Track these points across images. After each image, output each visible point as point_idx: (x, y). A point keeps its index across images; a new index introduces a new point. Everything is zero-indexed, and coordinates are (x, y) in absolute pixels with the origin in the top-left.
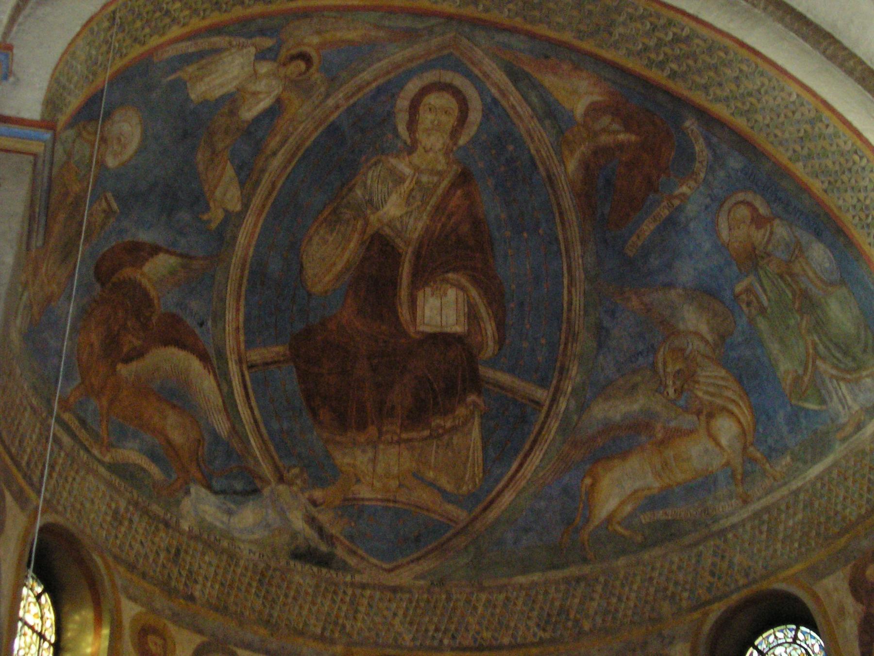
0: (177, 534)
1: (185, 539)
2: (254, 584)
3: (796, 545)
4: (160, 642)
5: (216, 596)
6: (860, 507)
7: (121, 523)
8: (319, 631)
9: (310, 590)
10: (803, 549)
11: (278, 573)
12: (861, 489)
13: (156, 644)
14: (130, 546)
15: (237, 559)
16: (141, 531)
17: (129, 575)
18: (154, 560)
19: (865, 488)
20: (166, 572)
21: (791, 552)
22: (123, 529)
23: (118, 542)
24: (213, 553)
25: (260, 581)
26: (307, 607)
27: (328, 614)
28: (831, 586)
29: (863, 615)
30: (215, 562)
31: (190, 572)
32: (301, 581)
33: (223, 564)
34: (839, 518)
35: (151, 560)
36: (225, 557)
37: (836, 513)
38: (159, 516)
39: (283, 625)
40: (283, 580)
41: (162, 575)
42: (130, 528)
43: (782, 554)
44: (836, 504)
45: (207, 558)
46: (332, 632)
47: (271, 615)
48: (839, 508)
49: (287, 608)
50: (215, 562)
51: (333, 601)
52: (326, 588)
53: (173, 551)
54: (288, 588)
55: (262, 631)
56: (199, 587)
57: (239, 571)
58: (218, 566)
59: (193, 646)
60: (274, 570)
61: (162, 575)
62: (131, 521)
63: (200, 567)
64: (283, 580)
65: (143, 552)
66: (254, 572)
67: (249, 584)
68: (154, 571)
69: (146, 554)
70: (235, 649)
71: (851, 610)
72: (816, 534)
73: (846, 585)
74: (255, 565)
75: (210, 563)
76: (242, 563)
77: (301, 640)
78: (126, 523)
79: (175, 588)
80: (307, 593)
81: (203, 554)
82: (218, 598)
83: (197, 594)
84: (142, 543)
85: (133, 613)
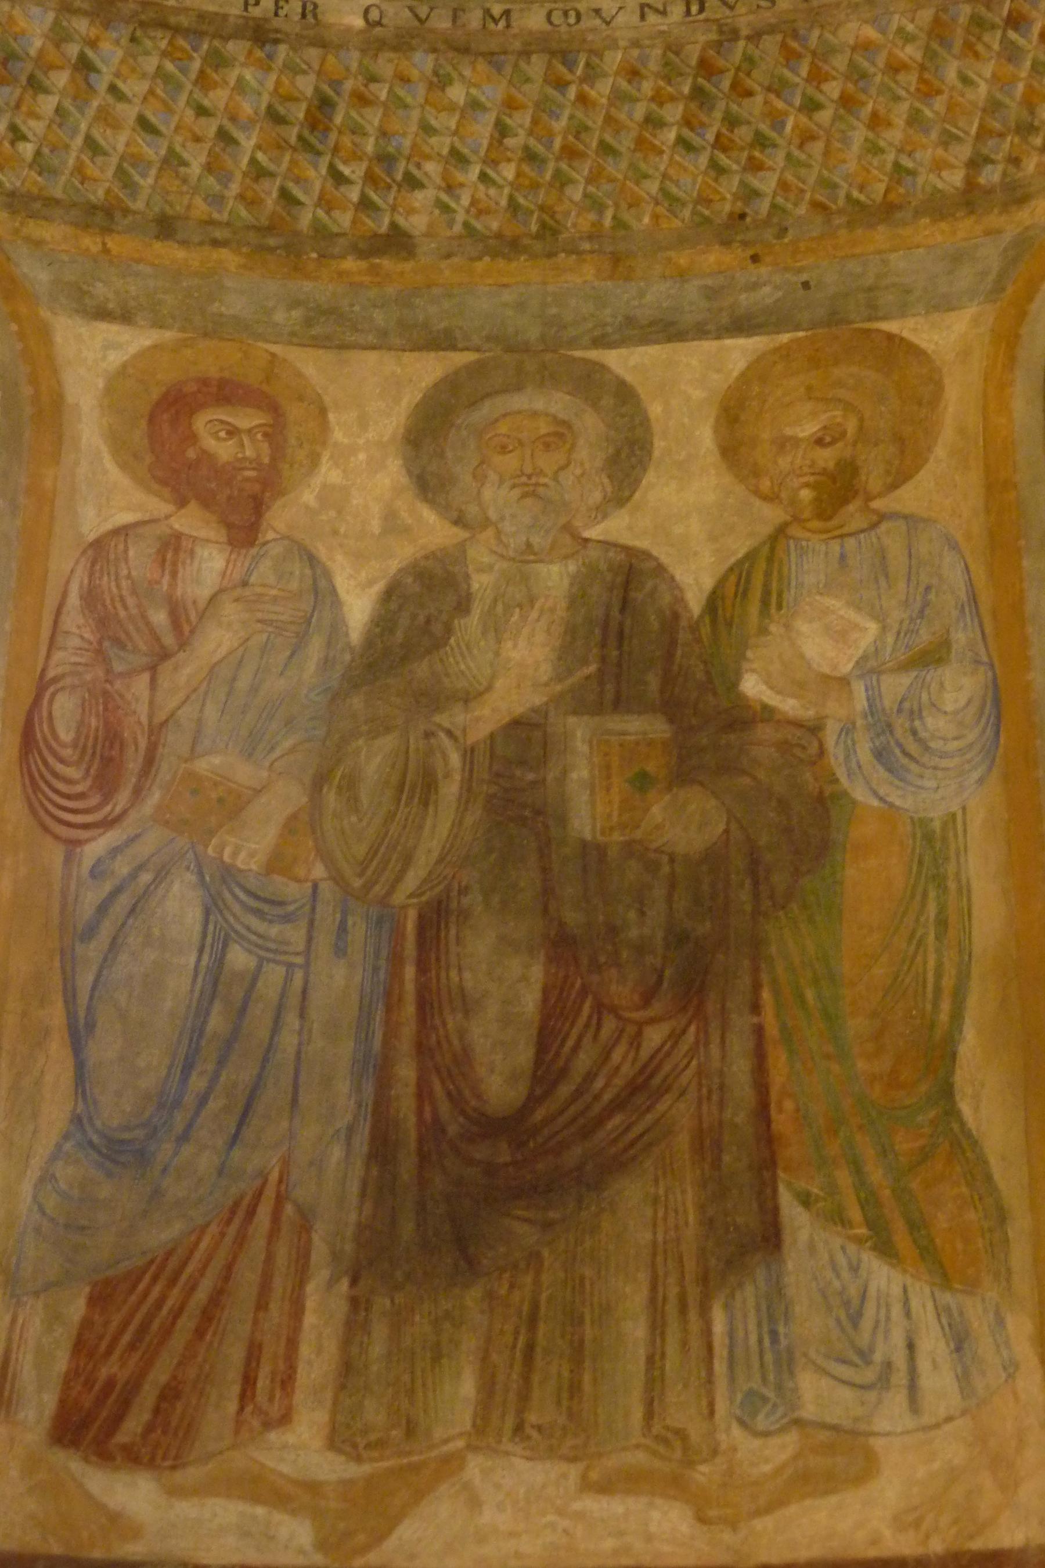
0: (313, 54)
1: (354, 58)
2: (673, 113)
4: (247, 419)
5: (504, 202)
7: (35, 85)
8: (956, 178)
9: (911, 52)
11: (770, 43)
13: (233, 432)
14: (91, 145)
15: (591, 51)
16: (135, 87)
17: (91, 242)
18: (209, 168)
20: (269, 193)
22: (47, 104)
23: (27, 149)
24: (482, 66)
25: (698, 92)
26: (900, 113)
27: (993, 106)
30: (493, 93)
31: (386, 159)
32: (870, 32)
33: (532, 91)
35: (195, 169)
36: (536, 67)
38: (225, 17)
39: (802, 210)
40: (791, 57)
41: (252, 203)
42: (80, 94)
45: (457, 93)
46: (1015, 161)
47: (752, 194)
49: (817, 148)
50: (493, 93)
51: (1011, 54)
52: (978, 22)
53: (299, 112)
54: (817, 77)
55: (714, 257)
56: (420, 198)
57: (601, 91)
58: (511, 105)
59: (410, 399)
60: (755, 37)
61: (252, 203)
62: (84, 66)
63: (427, 129)
64: (791, 57)
65: (152, 151)
66: (670, 72)
67: (653, 122)
68: (217, 200)
69: (171, 150)
70: (593, 354)
74: (674, 48)
75: (475, 105)
76: (614, 59)
77: (881, 235)
78: (61, 79)
79: (319, 231)
80: (895, 68)
81: (440, 82)
82: (513, 206)
83: (417, 224)
84: (144, 124)
85: (115, 359)
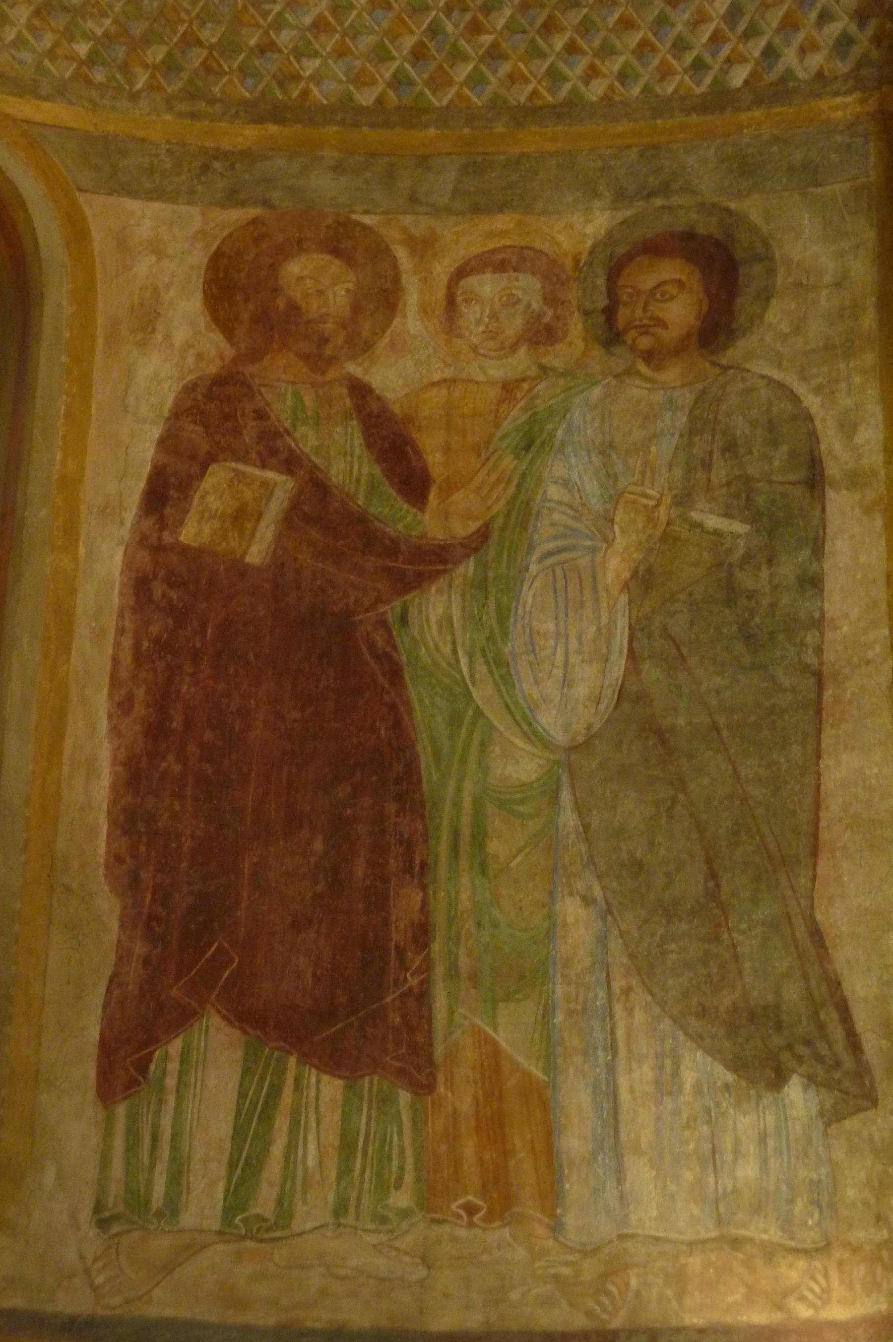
3: (82, 49)
6: (360, 80)
10: (99, 76)
12: (395, 37)
19: (408, 42)
21: (52, 54)
28: (145, 230)
29: (213, 369)
34: (270, 65)
37: (266, 48)
43: (19, 42)
44: (279, 24)
48: (285, 38)
71: (181, 336)
72: (163, 62)
73: (199, 258)
